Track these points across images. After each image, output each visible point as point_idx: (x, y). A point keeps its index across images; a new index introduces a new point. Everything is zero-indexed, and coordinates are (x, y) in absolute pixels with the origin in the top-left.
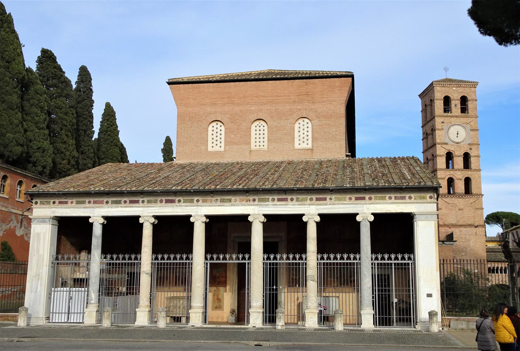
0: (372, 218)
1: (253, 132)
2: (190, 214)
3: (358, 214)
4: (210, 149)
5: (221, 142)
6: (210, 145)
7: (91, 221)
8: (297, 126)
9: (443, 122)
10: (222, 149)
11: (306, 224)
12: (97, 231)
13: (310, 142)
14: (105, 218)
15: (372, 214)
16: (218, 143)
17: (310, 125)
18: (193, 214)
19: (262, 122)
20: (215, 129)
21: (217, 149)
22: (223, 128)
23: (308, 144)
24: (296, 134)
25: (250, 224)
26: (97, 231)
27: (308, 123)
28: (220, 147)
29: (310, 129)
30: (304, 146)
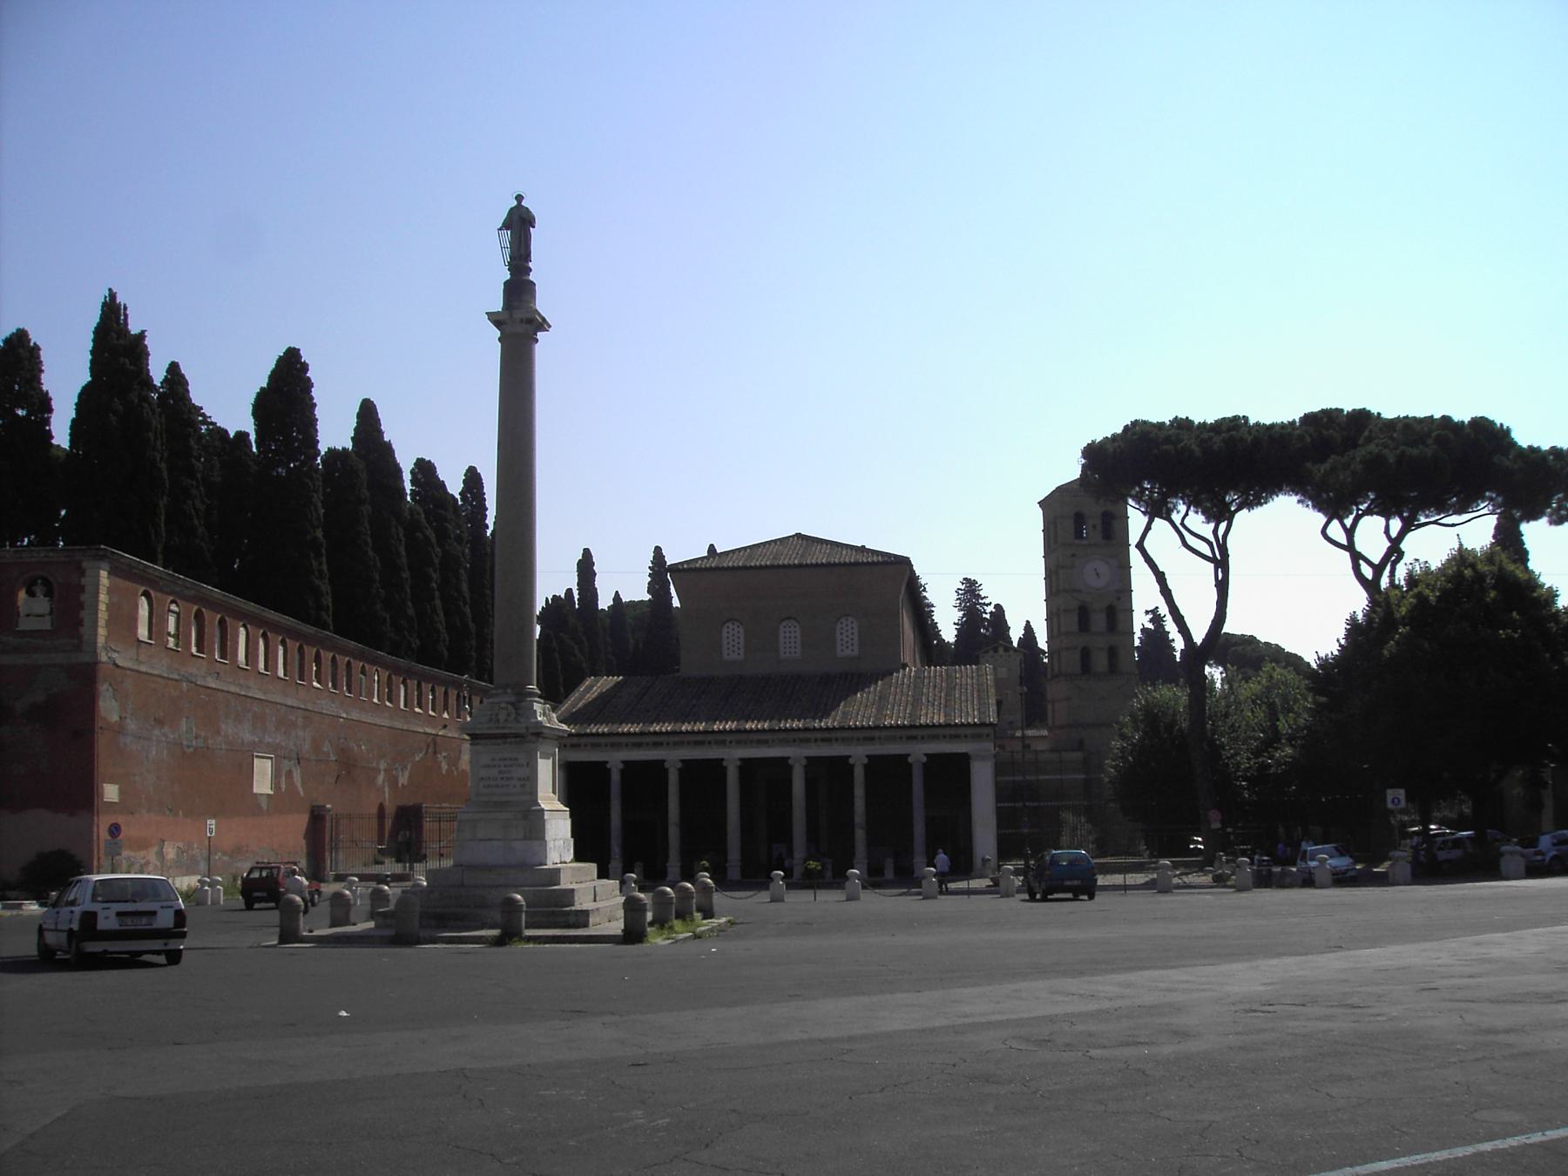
0: (925, 759)
1: (782, 635)
2: (721, 757)
3: (909, 755)
4: (725, 657)
5: (739, 649)
6: (725, 651)
7: (608, 766)
8: (839, 626)
9: (1073, 555)
10: (742, 657)
11: (852, 766)
12: (616, 777)
13: (856, 648)
14: (625, 762)
15: (926, 755)
16: (736, 649)
17: (855, 625)
18: (725, 757)
19: (793, 622)
20: (730, 630)
21: (734, 656)
22: (741, 630)
23: (853, 650)
24: (839, 637)
25: (790, 768)
26: (616, 777)
27: (852, 623)
28: (739, 654)
29: (856, 631)
30: (848, 652)
